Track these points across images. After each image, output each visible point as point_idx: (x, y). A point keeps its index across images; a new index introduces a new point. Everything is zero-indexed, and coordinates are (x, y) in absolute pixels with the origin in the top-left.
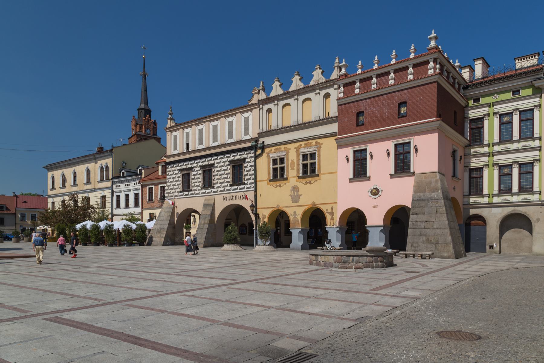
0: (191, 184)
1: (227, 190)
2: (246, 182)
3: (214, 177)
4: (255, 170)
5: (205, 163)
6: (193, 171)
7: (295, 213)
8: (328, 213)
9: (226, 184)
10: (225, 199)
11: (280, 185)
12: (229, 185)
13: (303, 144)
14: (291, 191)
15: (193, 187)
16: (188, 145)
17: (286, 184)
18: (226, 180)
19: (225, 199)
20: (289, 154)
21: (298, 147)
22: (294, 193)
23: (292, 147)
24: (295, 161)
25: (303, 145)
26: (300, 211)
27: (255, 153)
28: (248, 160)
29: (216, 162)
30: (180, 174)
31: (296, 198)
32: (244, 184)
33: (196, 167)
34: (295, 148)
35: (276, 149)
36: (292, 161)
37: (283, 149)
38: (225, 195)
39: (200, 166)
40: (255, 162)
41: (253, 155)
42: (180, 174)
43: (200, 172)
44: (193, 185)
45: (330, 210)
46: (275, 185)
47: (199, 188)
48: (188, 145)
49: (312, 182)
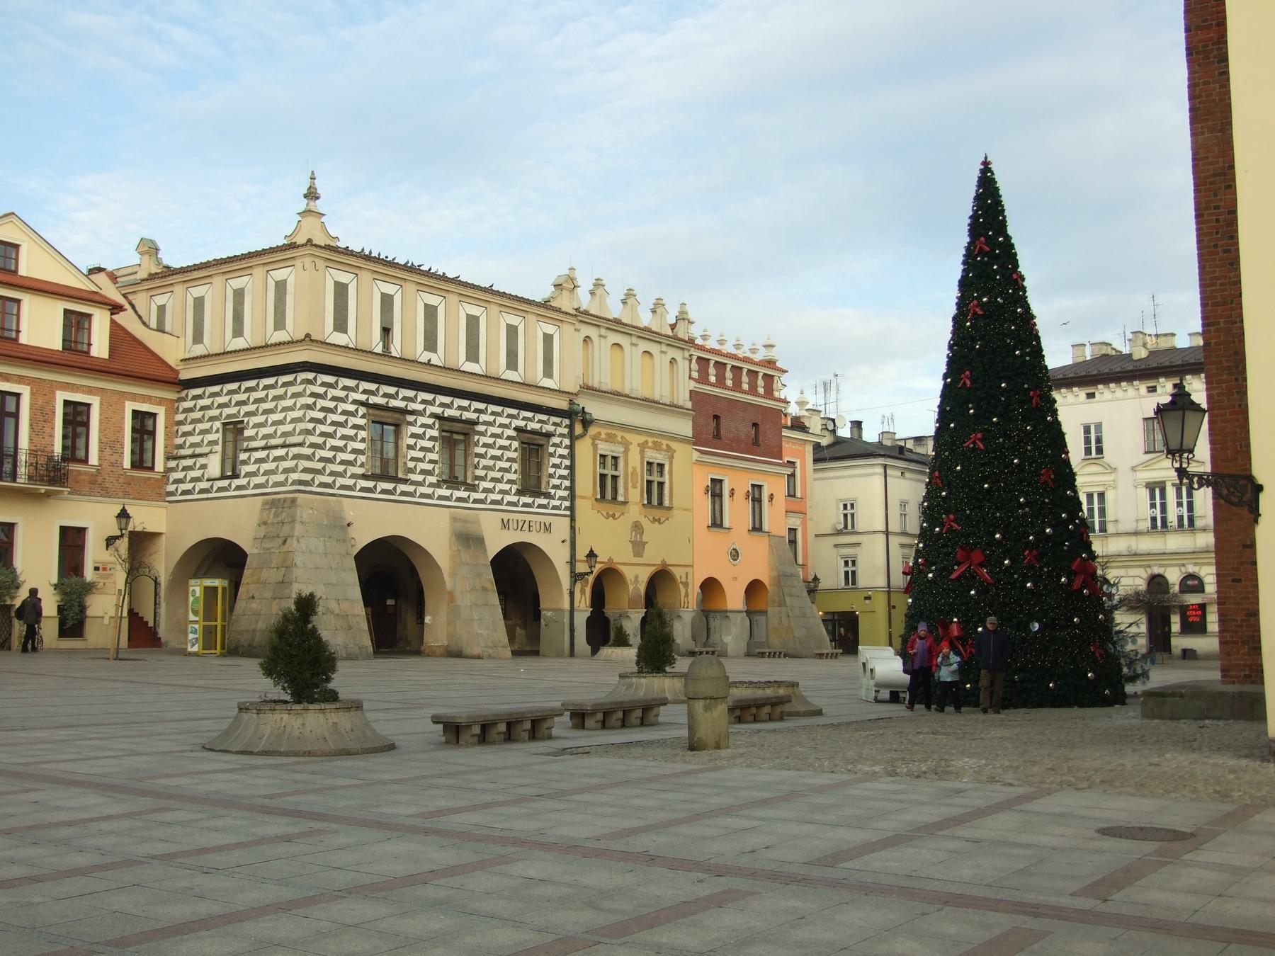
1: (509, 504)
2: (552, 491)
3: (476, 460)
4: (571, 468)
5: (449, 413)
7: (636, 577)
8: (682, 583)
9: (507, 487)
10: (505, 525)
12: (514, 491)
13: (650, 440)
14: (632, 532)
15: (412, 471)
16: (386, 331)
19: (505, 525)
20: (629, 453)
21: (643, 443)
22: (636, 536)
23: (635, 439)
24: (639, 470)
25: (650, 444)
26: (644, 575)
27: (571, 427)
28: (556, 440)
29: (481, 420)
30: (363, 416)
31: (638, 547)
34: (639, 445)
35: (609, 435)
36: (634, 468)
38: (506, 516)
39: (434, 416)
40: (571, 447)
41: (566, 431)
42: (364, 416)
43: (435, 433)
44: (411, 464)
45: (684, 580)
47: (433, 479)
48: (386, 331)
49: (663, 519)
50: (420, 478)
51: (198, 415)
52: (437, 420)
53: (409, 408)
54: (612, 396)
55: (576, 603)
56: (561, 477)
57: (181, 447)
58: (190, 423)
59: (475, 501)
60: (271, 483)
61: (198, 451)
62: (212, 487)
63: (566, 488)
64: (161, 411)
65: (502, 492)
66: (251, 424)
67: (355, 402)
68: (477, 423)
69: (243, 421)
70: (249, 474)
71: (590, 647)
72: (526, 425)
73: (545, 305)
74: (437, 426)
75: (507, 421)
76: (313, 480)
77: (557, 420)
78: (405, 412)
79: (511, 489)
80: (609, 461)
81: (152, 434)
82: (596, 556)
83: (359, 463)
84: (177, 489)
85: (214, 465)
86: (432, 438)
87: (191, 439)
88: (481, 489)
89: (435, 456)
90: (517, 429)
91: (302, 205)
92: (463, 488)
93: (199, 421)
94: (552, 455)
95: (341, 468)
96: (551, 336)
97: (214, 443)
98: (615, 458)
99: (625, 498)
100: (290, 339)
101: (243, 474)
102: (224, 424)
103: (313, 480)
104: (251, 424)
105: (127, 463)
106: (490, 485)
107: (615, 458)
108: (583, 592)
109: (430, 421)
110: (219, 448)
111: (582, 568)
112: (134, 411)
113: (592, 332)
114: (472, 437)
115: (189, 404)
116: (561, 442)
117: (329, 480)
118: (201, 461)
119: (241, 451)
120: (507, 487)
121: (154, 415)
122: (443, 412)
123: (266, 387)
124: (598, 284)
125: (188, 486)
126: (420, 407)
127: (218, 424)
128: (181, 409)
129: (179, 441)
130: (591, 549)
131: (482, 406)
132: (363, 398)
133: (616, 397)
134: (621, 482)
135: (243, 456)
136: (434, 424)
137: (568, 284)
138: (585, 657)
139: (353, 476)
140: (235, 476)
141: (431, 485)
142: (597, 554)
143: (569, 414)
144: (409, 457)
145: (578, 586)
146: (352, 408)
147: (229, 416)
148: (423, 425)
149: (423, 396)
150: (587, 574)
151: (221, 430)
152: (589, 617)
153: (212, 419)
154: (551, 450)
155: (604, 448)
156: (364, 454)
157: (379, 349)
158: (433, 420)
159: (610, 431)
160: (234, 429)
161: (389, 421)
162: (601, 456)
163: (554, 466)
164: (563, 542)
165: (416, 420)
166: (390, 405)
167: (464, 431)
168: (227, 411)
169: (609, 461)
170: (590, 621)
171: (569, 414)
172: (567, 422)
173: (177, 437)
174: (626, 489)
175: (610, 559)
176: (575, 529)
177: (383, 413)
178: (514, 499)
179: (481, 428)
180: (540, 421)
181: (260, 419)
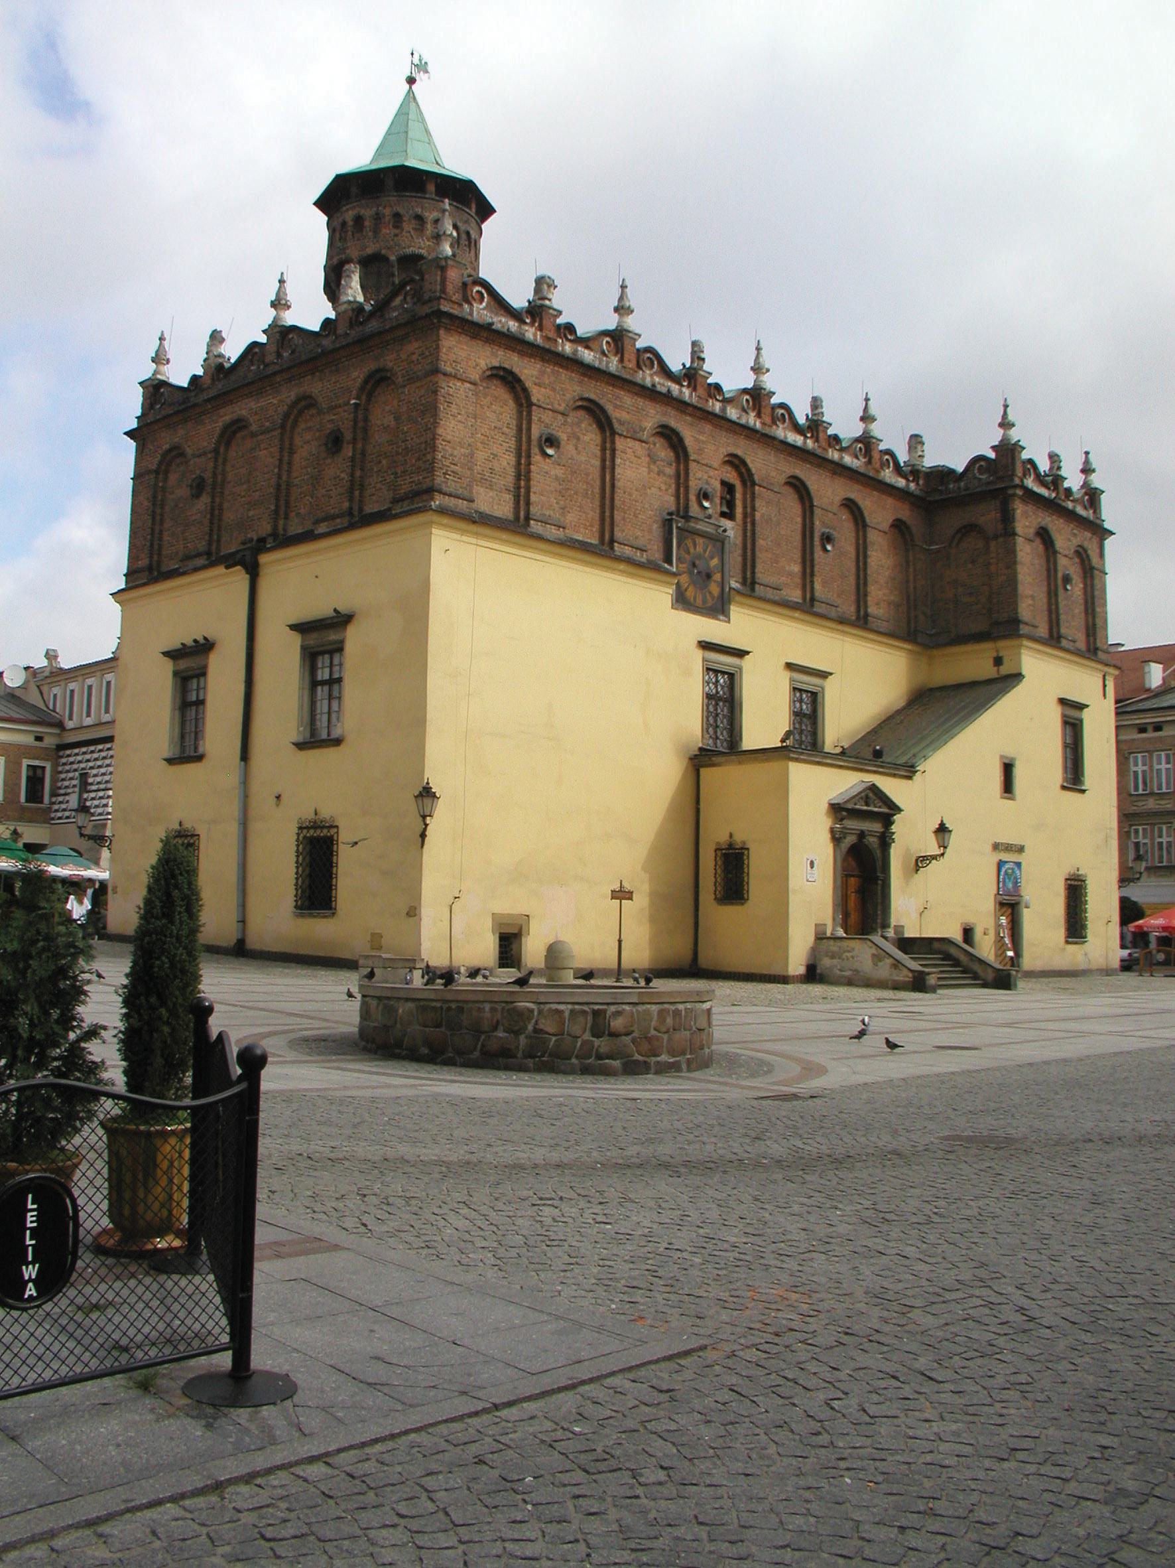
51: (67, 768)
57: (60, 788)
61: (69, 791)
64: (48, 766)
81: (42, 780)
87: (66, 783)
97: (74, 786)
102: (81, 774)
105: (23, 798)
110: (77, 789)
112: (28, 766)
115: (64, 760)
118: (67, 798)
121: (43, 768)
125: (59, 814)
127: (77, 774)
135: (85, 796)
147: (83, 769)
153: (75, 770)
160: (84, 776)
168: (82, 765)
181: (94, 772)
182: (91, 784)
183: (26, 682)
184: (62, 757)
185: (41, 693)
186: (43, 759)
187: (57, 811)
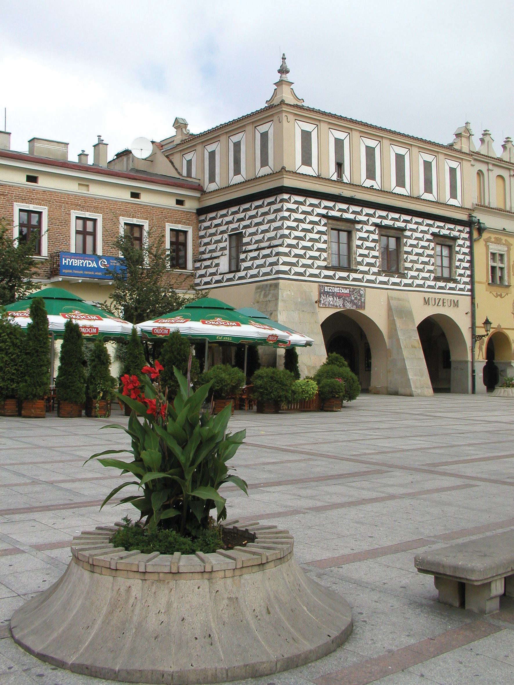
0: (354, 256)
1: (429, 287)
3: (405, 256)
4: (471, 262)
5: (385, 222)
6: (358, 230)
9: (427, 275)
10: (426, 302)
11: (502, 295)
12: (432, 278)
16: (339, 166)
17: (507, 294)
18: (428, 267)
19: (426, 302)
20: (511, 251)
27: (470, 233)
29: (408, 228)
30: (325, 225)
32: (455, 281)
33: (366, 223)
35: (495, 238)
37: (504, 242)
38: (427, 296)
39: (376, 225)
40: (471, 247)
41: (467, 236)
42: (325, 225)
44: (359, 259)
46: (495, 293)
47: (375, 270)
48: (339, 166)
50: (366, 269)
51: (213, 231)
52: (377, 228)
53: (357, 219)
54: (498, 211)
55: (476, 357)
56: (464, 268)
57: (203, 253)
58: (209, 237)
59: (406, 285)
60: (261, 274)
61: (215, 254)
62: (223, 278)
63: (468, 276)
65: (424, 278)
66: (247, 234)
67: (318, 215)
68: (405, 230)
69: (242, 232)
70: (247, 269)
71: (485, 387)
72: (439, 232)
73: (450, 147)
74: (377, 232)
75: (426, 228)
76: (290, 270)
77: (461, 228)
78: (354, 222)
79: (430, 276)
80: (498, 258)
81: (185, 245)
82: (490, 323)
83: (322, 258)
84: (201, 282)
85: (224, 264)
86: (374, 241)
88: (409, 276)
89: (376, 254)
90: (433, 234)
91: (277, 77)
92: (396, 276)
93: (214, 234)
94: (458, 253)
95: (310, 262)
96: (455, 170)
97: (224, 249)
98: (501, 256)
99: (508, 283)
100: (271, 172)
101: (242, 268)
102: (230, 236)
103: (290, 270)
104: (247, 234)
106: (415, 274)
107: (501, 256)
108: (480, 349)
109: (372, 228)
110: (227, 252)
111: (480, 331)
112: (171, 230)
113: (483, 168)
114: (402, 240)
116: (464, 244)
117: (302, 270)
118: (216, 261)
119: (241, 252)
120: (427, 275)
121: (185, 233)
122: (381, 222)
123: (257, 207)
124: (486, 133)
126: (365, 219)
127: (226, 236)
128: (202, 228)
129: (202, 249)
130: (487, 318)
131: (408, 218)
132: (324, 212)
133: (500, 212)
134: (506, 271)
135: (242, 256)
136: (375, 230)
137: (466, 133)
138: (482, 393)
139: (319, 267)
140: (238, 270)
141: (374, 274)
142: (491, 322)
143: (469, 223)
144: (358, 254)
145: (478, 344)
146: (317, 219)
147: (233, 230)
148: (367, 231)
149: (366, 210)
150: (484, 336)
151: (228, 240)
152: (485, 366)
153: (222, 232)
154: (457, 249)
155: (494, 248)
156: (326, 252)
157: (335, 177)
158: (375, 228)
159: (497, 236)
161: (343, 228)
162: (491, 253)
163: (460, 260)
164: (466, 314)
165: (362, 228)
166: (344, 217)
167: (396, 235)
168: (232, 226)
169: (498, 258)
170: (485, 369)
171: (469, 223)
172: (467, 229)
173: (200, 247)
174: (509, 277)
175: (499, 326)
176: (474, 304)
177: (339, 223)
178: (432, 283)
179: (408, 233)
180: (449, 229)
181: (253, 230)
182: (248, 244)
183: (153, 154)
184: (204, 221)
185: (172, 163)
186: (184, 223)
187: (202, 276)
